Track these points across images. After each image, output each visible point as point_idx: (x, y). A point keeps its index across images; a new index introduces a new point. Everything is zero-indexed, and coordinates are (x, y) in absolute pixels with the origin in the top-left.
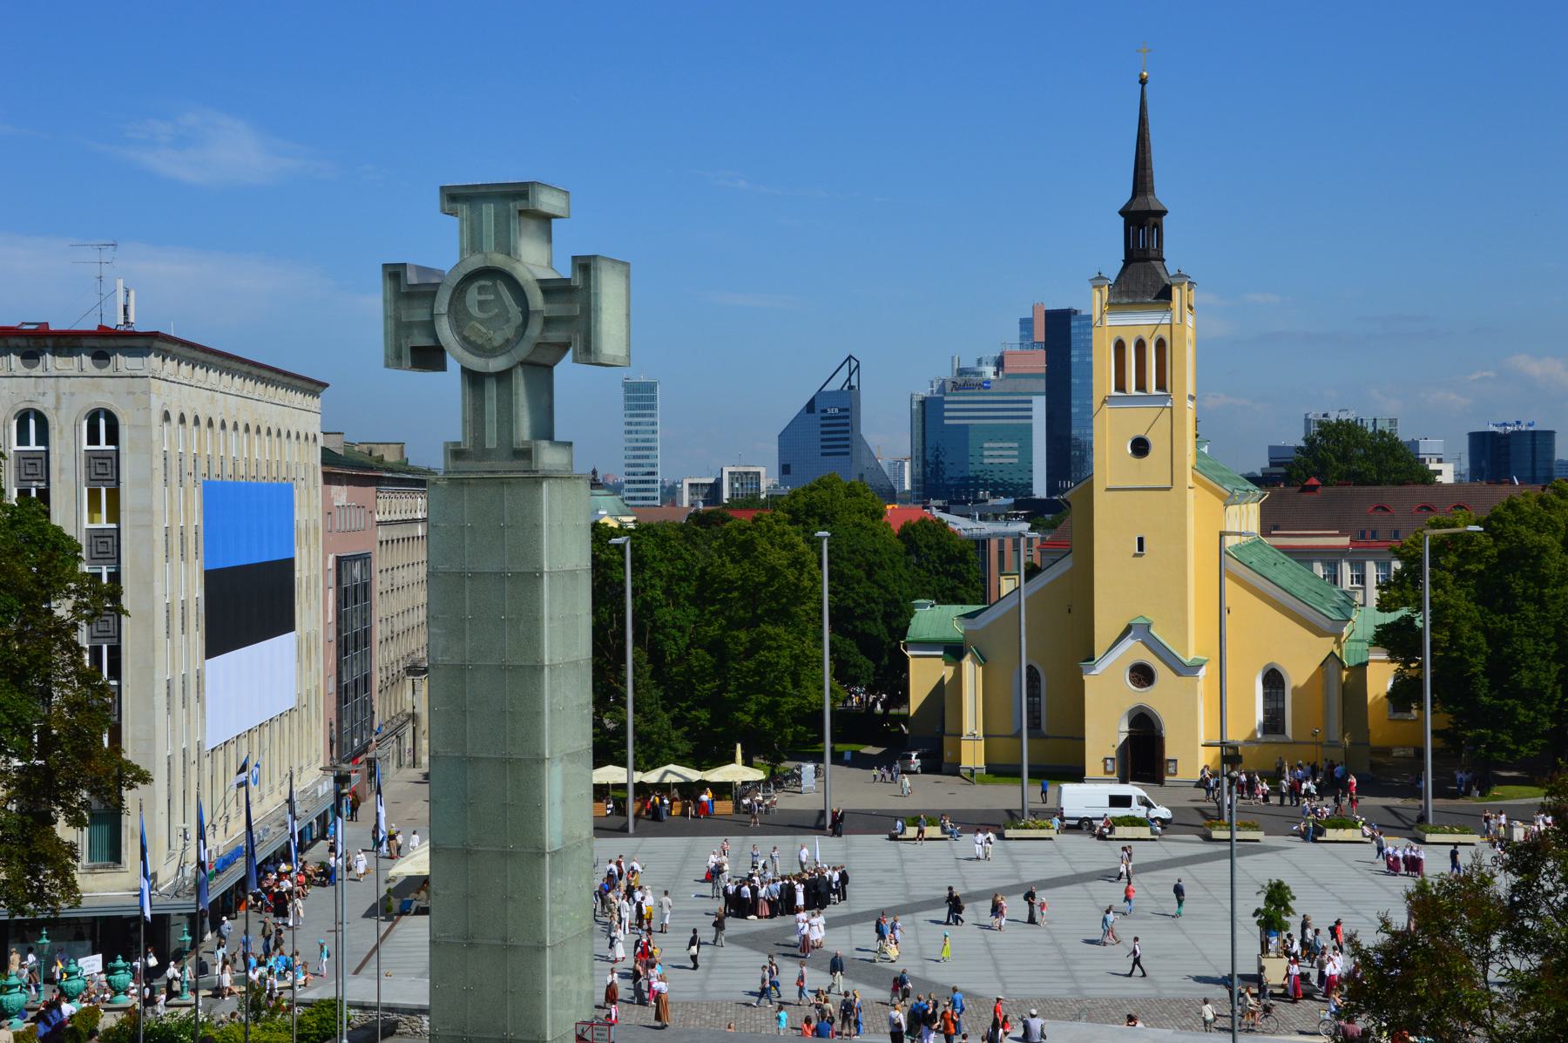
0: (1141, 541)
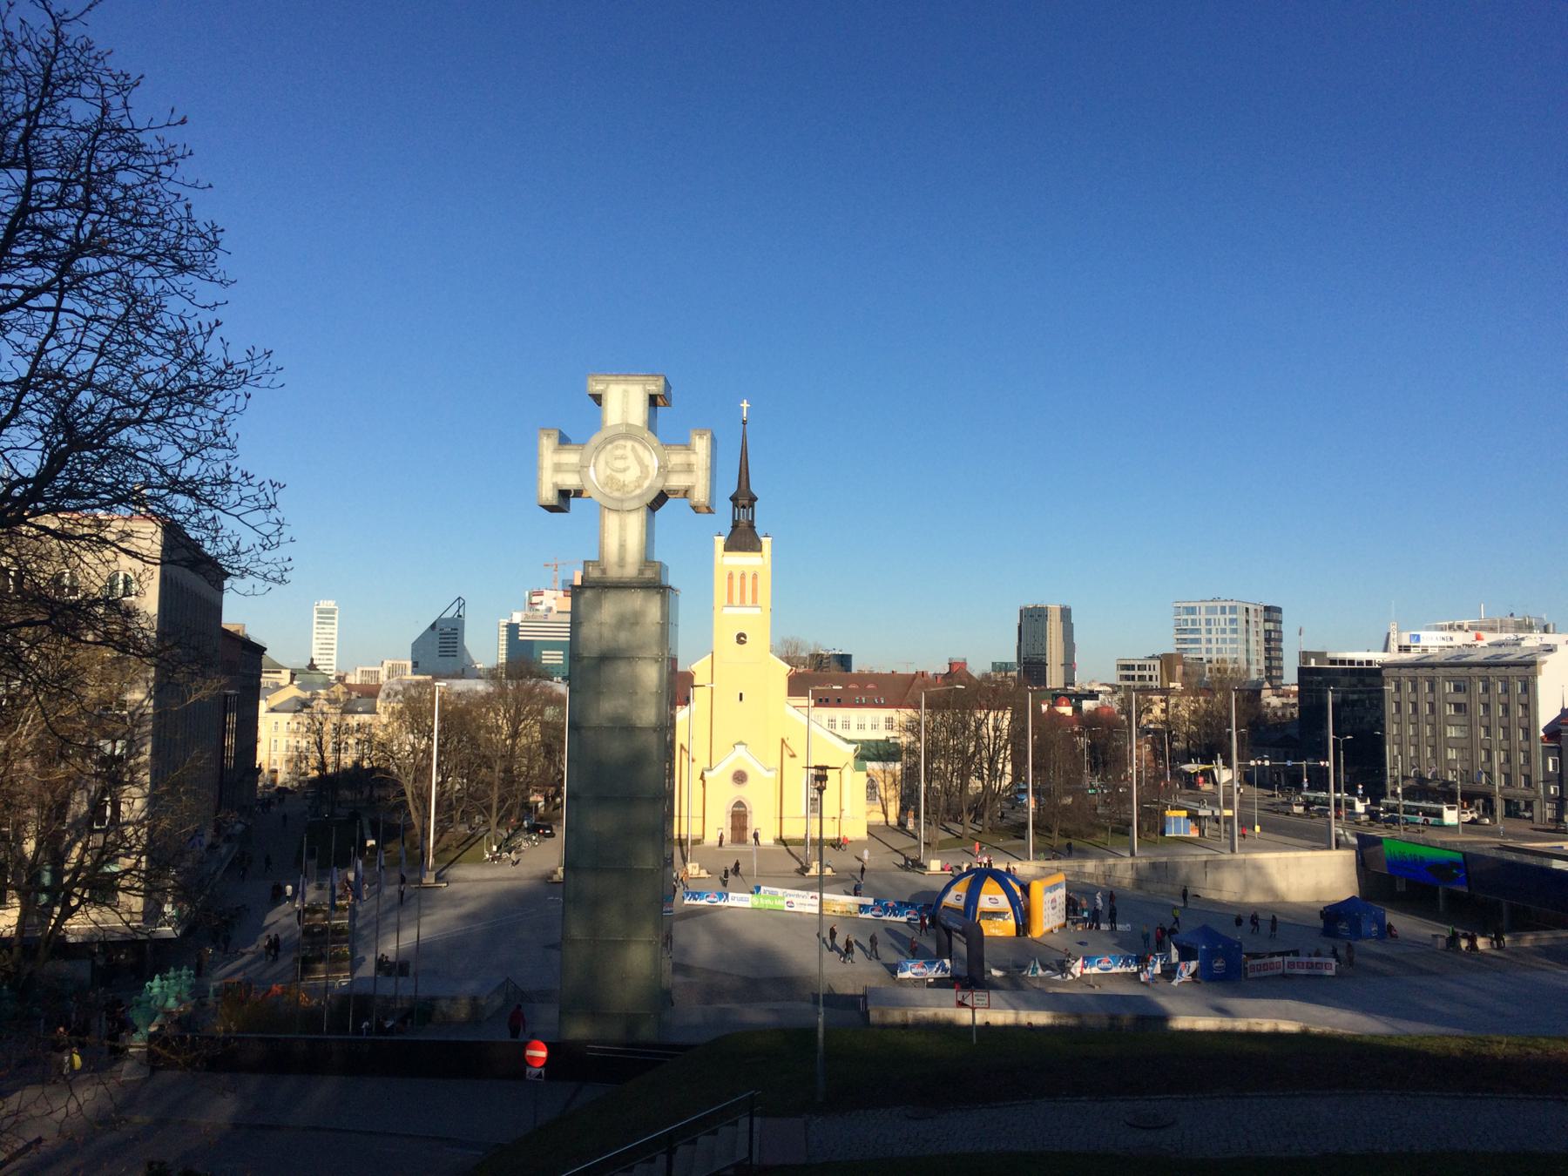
0: (741, 695)
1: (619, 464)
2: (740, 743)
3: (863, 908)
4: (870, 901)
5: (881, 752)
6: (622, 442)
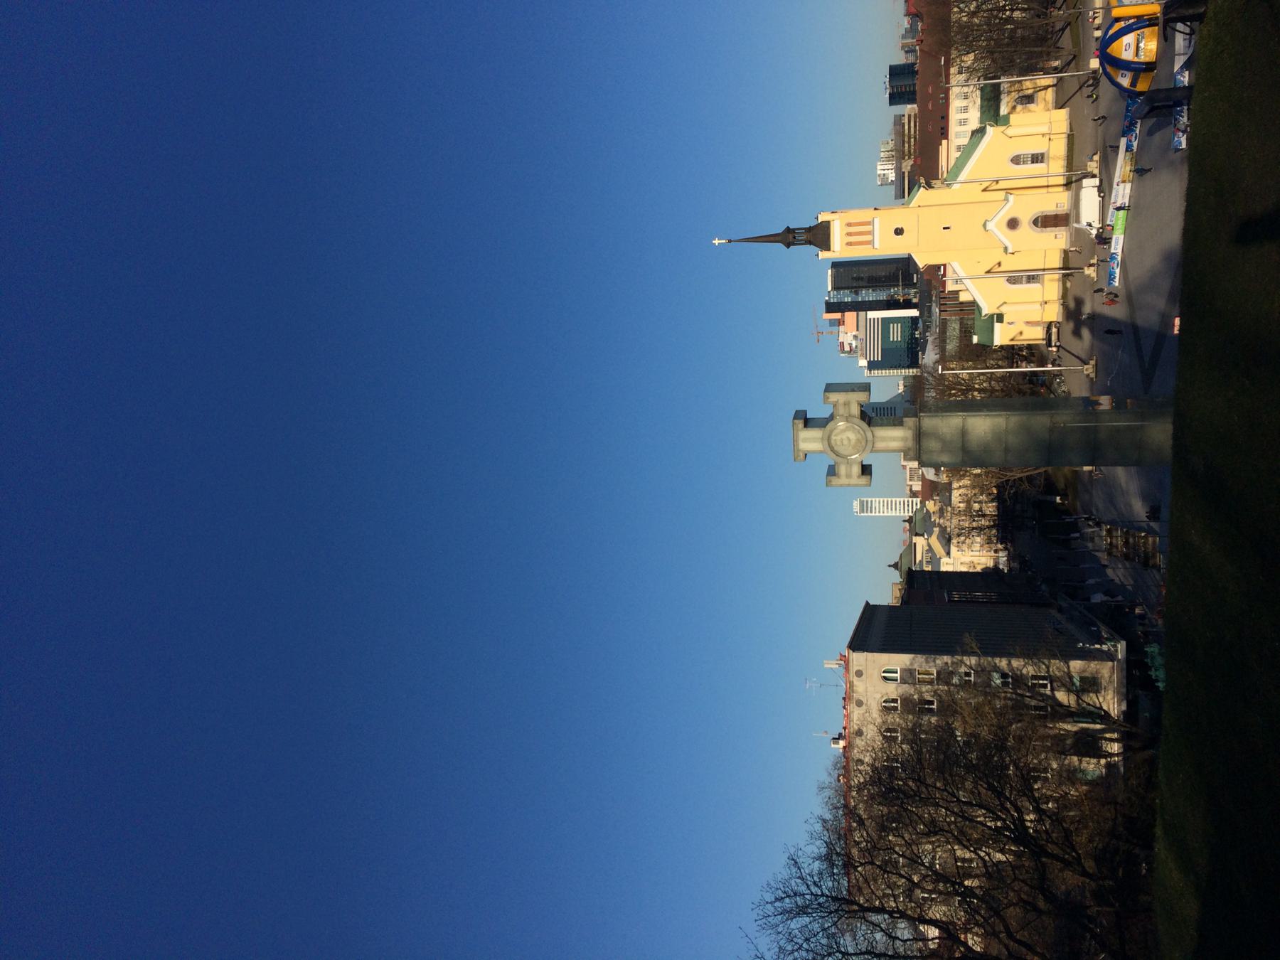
0: (944, 228)
1: (845, 442)
2: (985, 225)
3: (1129, 148)
4: (1123, 141)
5: (993, 95)
6: (833, 442)
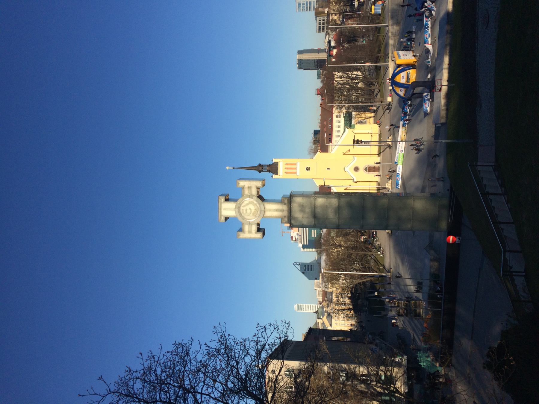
0: (327, 169)
1: (249, 211)
2: (344, 169)
3: (404, 125)
4: (401, 123)
5: (349, 119)
6: (241, 211)
